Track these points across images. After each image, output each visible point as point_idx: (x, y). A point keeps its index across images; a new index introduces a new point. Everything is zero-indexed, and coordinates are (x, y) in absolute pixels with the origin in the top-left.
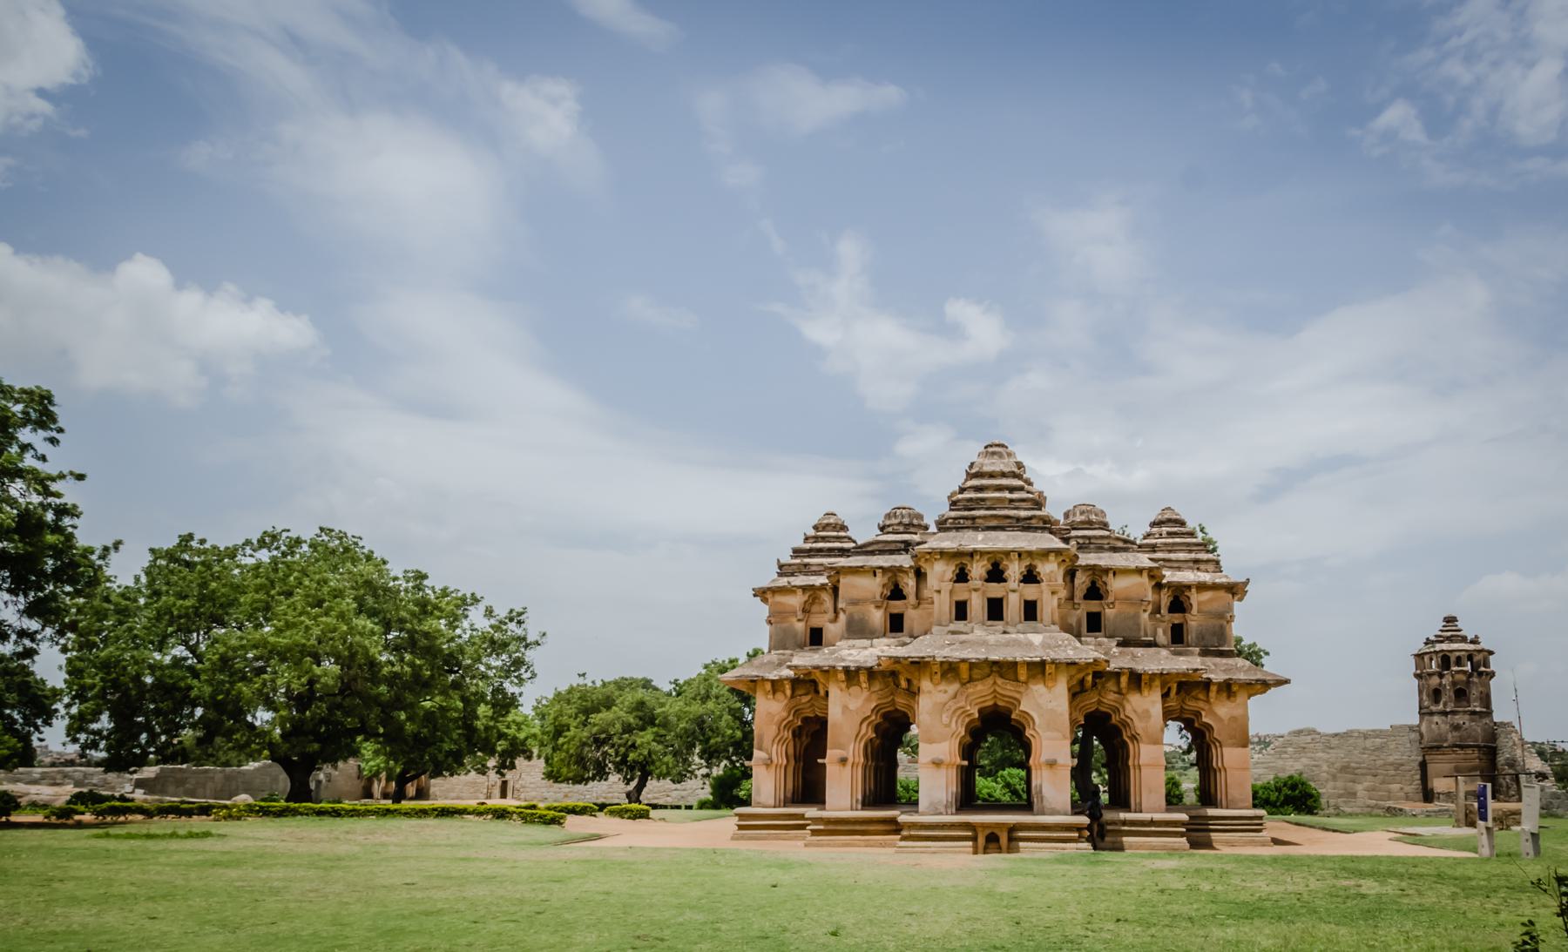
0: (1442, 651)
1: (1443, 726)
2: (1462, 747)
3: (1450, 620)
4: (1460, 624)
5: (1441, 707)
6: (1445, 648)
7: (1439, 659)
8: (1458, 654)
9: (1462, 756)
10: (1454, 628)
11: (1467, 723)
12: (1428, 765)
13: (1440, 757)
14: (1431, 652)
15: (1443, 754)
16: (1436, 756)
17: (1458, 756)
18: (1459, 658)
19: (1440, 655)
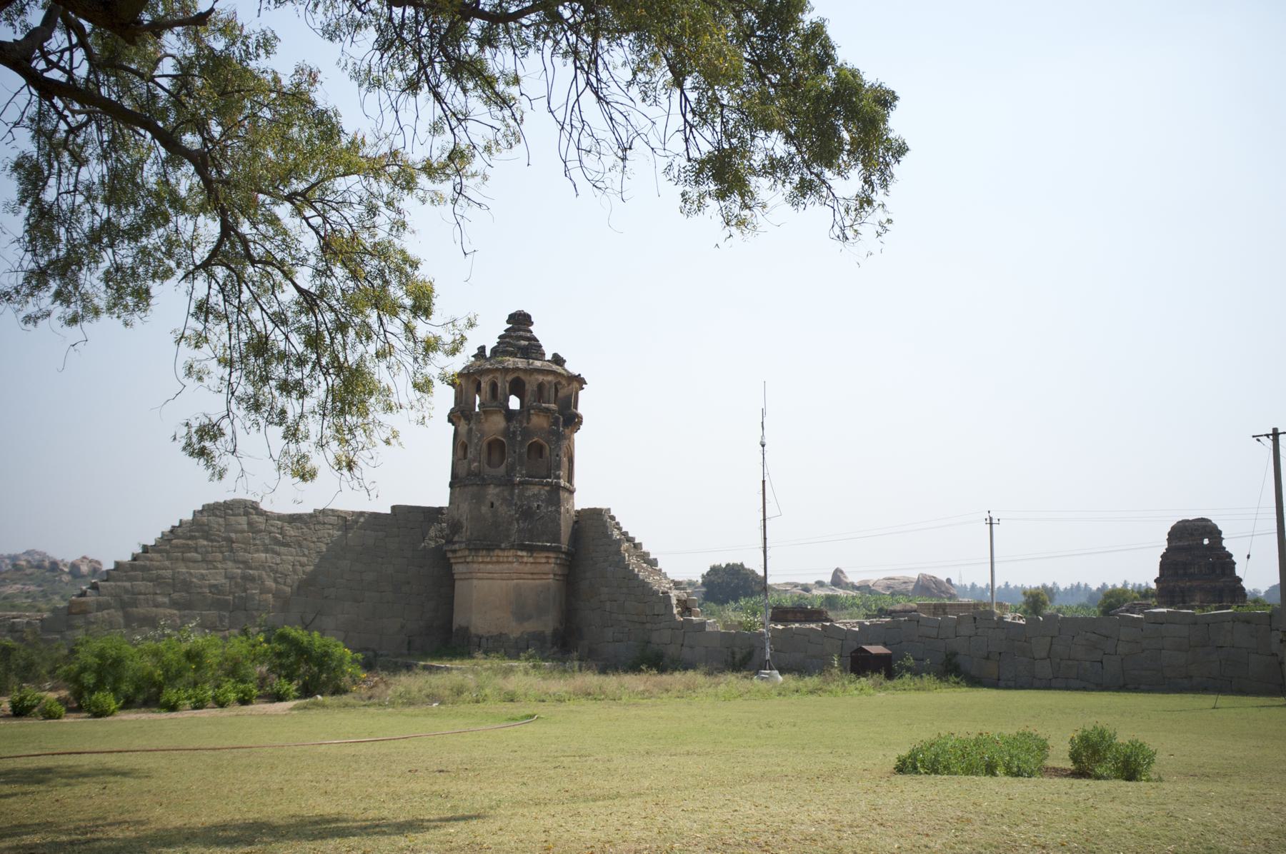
0: (518, 369)
1: (502, 509)
2: (531, 549)
3: (520, 321)
4: (536, 330)
5: (502, 470)
6: (520, 365)
7: (507, 385)
8: (541, 378)
9: (528, 568)
10: (529, 335)
11: (543, 509)
12: (458, 584)
13: (490, 566)
14: (497, 369)
15: (498, 562)
16: (482, 566)
17: (521, 567)
18: (541, 386)
19: (509, 378)
